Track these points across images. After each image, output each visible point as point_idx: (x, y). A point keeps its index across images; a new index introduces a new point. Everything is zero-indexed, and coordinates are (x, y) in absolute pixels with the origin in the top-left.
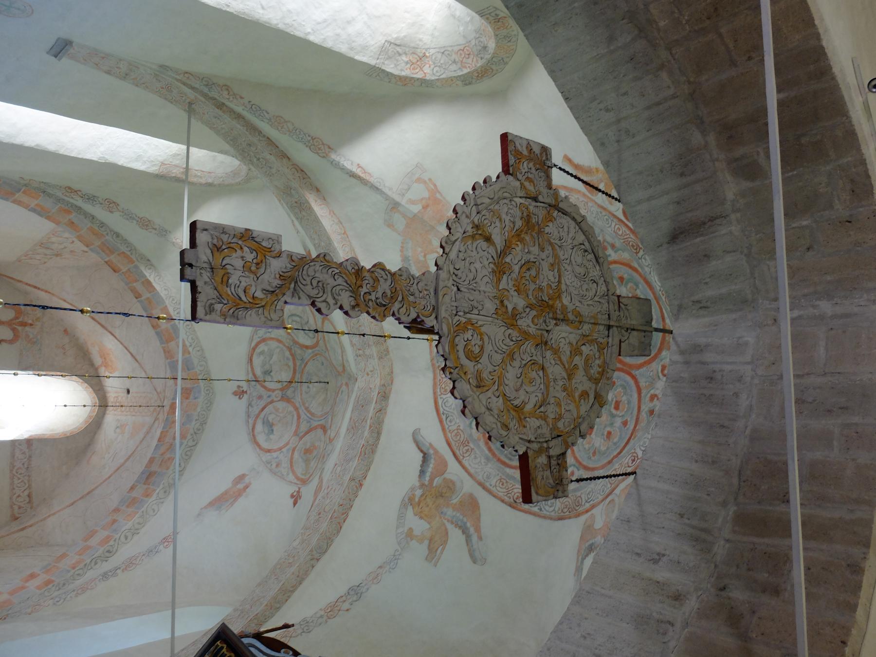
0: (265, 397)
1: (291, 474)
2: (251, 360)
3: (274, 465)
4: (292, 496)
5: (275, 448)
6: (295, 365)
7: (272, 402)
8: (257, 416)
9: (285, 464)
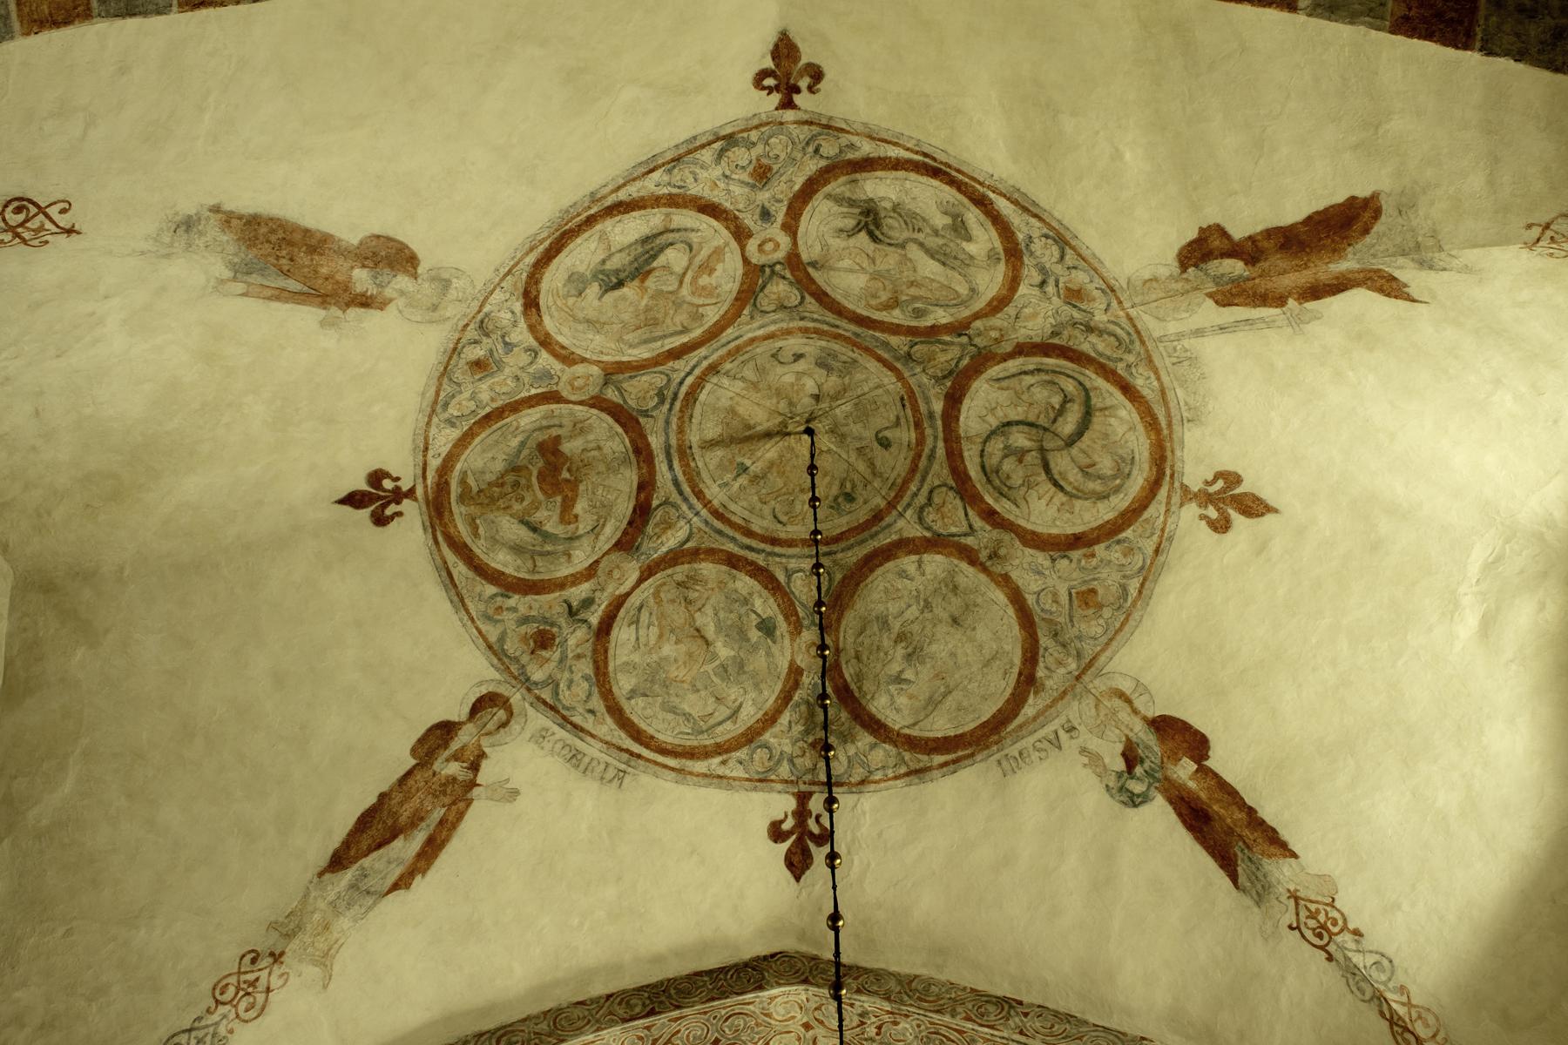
0: (763, 196)
1: (455, 434)
2: (935, 173)
3: (478, 352)
4: (376, 477)
5: (549, 324)
6: (895, 329)
7: (741, 235)
8: (674, 201)
9: (490, 392)
